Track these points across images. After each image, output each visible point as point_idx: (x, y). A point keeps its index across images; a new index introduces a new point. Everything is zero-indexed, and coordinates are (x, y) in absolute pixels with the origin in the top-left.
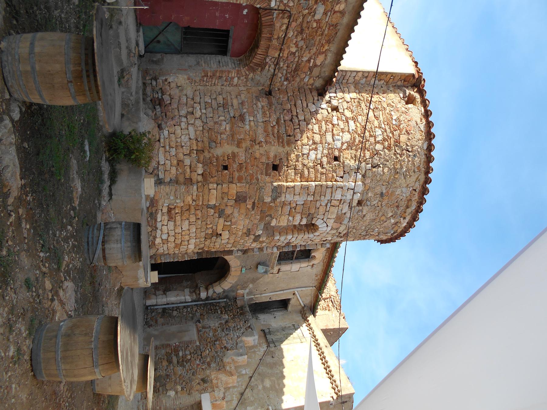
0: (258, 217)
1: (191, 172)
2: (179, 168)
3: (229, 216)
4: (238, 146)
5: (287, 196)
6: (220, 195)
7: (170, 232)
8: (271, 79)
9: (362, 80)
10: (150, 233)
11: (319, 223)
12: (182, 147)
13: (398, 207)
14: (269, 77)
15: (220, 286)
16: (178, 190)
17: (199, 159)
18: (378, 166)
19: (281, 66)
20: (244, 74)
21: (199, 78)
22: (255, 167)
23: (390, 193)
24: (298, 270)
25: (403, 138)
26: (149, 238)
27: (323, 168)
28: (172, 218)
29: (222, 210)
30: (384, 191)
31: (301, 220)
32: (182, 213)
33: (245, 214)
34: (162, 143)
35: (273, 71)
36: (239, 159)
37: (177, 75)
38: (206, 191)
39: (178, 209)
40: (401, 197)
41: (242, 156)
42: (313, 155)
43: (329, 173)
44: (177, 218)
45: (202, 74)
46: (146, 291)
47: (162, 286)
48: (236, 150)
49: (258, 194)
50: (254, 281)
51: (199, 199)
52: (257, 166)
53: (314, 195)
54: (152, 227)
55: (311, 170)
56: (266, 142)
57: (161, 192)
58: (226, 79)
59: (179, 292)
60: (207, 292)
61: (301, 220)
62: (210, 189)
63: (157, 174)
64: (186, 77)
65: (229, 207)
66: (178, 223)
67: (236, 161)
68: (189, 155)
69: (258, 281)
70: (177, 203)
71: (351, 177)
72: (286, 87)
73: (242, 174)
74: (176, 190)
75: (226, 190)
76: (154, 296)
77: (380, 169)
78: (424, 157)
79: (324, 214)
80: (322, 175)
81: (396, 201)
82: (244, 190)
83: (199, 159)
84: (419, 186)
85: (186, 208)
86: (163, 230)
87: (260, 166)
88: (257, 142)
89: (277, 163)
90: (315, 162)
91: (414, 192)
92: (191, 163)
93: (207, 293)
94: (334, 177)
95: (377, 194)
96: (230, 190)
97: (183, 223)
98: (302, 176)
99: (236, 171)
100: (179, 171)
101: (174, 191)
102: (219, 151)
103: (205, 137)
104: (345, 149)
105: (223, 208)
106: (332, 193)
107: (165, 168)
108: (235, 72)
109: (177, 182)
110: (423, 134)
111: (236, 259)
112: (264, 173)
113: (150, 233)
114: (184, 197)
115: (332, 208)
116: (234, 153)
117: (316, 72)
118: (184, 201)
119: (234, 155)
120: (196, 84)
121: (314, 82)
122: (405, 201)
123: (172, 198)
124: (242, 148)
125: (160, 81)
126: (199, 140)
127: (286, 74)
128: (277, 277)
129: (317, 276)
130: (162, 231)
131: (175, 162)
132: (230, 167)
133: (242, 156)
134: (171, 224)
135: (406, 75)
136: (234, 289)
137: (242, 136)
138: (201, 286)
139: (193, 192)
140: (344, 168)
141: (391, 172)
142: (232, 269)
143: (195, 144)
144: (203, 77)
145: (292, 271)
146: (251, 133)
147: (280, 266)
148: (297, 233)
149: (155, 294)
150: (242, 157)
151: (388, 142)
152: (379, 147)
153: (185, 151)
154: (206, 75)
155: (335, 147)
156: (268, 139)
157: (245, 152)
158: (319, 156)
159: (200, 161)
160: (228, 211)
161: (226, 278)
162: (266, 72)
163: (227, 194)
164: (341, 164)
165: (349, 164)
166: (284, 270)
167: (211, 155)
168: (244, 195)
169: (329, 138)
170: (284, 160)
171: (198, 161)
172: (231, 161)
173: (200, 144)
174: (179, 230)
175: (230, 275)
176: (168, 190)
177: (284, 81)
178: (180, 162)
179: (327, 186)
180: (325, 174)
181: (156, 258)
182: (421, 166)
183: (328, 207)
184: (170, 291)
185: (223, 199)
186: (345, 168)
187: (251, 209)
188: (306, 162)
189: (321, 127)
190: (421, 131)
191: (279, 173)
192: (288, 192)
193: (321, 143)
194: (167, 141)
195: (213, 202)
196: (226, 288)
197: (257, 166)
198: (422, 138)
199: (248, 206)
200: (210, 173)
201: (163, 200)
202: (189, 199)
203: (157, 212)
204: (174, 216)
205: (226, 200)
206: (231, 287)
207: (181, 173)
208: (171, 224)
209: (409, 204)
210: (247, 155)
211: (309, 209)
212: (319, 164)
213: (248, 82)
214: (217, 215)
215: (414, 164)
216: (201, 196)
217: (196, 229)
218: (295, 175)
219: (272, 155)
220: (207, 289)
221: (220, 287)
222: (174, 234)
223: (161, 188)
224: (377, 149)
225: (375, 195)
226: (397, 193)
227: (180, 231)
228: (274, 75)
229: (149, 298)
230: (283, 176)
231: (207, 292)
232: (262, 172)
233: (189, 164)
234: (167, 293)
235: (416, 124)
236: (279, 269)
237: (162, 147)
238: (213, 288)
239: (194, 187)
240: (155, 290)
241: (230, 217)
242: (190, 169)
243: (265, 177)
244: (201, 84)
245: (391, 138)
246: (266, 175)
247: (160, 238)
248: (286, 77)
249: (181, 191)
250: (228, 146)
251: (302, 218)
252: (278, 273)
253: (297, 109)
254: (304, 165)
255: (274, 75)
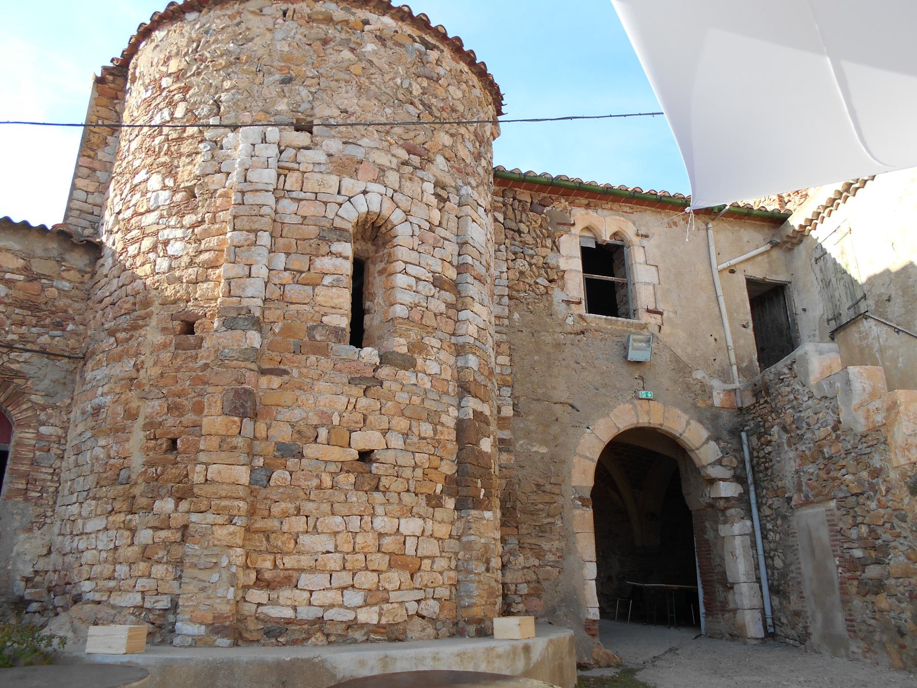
0: (313, 358)
1: (169, 528)
2: (156, 557)
3: (299, 432)
4: (132, 416)
5: (249, 292)
6: (223, 455)
7: (335, 584)
8: (52, 357)
9: (98, 177)
10: (332, 638)
11: (350, 215)
12: (116, 548)
13: (325, 42)
14: (46, 360)
15: (698, 449)
16: (195, 560)
17: (143, 508)
18: (217, 103)
19: (15, 337)
20: (30, 413)
21: (30, 508)
22: (179, 375)
23: (283, 64)
24: (654, 268)
25: (174, 66)
26: (355, 641)
27: (203, 221)
28: (288, 578)
29: (278, 450)
30: (278, 77)
31: (339, 255)
32: (275, 550)
33: (298, 392)
34: (102, 596)
35: (27, 355)
36: (157, 413)
37: (14, 554)
38: (208, 489)
39: (260, 561)
40: (298, 36)
41: (153, 407)
42: (175, 248)
43: (215, 205)
44: (288, 566)
45: (19, 502)
46: (731, 635)
47: (718, 591)
48: (141, 421)
49: (235, 362)
50: (682, 368)
51: (225, 507)
52: (178, 370)
53: (256, 232)
54: (311, 632)
55: (202, 247)
56: (137, 354)
57: (195, 606)
58: (40, 449)
59: (725, 550)
60: (720, 480)
61: (339, 255)
62: (207, 480)
63: (161, 612)
64: (22, 536)
65: (272, 432)
66: (306, 561)
67: (161, 420)
68: (133, 531)
69: (685, 359)
70: (230, 563)
71: (228, 156)
72: (81, 324)
73: (187, 403)
74: (194, 566)
75: (215, 441)
76: (739, 615)
77: (224, 96)
78: (212, 13)
79: (325, 203)
80: (217, 220)
81: (307, 47)
82: (218, 397)
83: (143, 508)
84: (274, 6)
85: (261, 542)
86: (327, 602)
87: (178, 362)
88: (134, 375)
89: (177, 325)
90: (190, 239)
91: (290, 13)
92: (150, 528)
93: (724, 480)
94: (226, 192)
95: (283, 91)
96: (213, 432)
97: (307, 548)
98: (213, 264)
99: (182, 419)
100: (163, 557)
101: (196, 573)
102: (137, 461)
103: (108, 494)
104: (175, 182)
105: (271, 449)
106: (257, 191)
107: (150, 593)
108: (22, 432)
109: (179, 563)
110: (173, 28)
111: (611, 415)
112: (194, 352)
113: (332, 638)
114: (215, 546)
115: (308, 186)
116: (144, 425)
117: (38, 267)
118: (228, 546)
119: (150, 425)
120: (49, 514)
121: (73, 268)
122: (312, 27)
123: (215, 577)
124: (139, 407)
125: (28, 593)
126: (109, 508)
127: (43, 326)
128: (672, 315)
129: (675, 224)
130: (332, 606)
131: (142, 566)
132: (170, 432)
133: (153, 407)
134: (305, 580)
135: (97, 95)
136: (710, 418)
137: (120, 409)
138: (708, 495)
139: (206, 522)
140: (207, 175)
141: (233, 72)
142: (643, 421)
143: (114, 518)
144: (27, 499)
145: (656, 281)
146: (117, 390)
147: (640, 311)
148: (395, 264)
149: (735, 611)
150: (153, 407)
151: (174, 95)
152: (180, 112)
153: (125, 541)
154: (24, 492)
155: (168, 202)
156: (132, 351)
157: (147, 401)
158: (179, 233)
159: (148, 505)
160: (283, 433)
161: (675, 436)
162: (28, 367)
163: (223, 438)
164: (199, 183)
165: (199, 166)
166: (653, 299)
167: (140, 481)
168: (231, 395)
169: (151, 218)
170: (173, 309)
171: (149, 509)
172: (158, 432)
173: (117, 505)
174: (333, 562)
175: (662, 425)
176: (191, 587)
177: (64, 330)
178: (146, 555)
179: (240, 204)
180: (215, 213)
181: (465, 621)
182: (229, 12)
183: (302, 195)
184: (725, 572)
185: (236, 448)
186: (207, 172)
187: (286, 377)
188: (186, 260)
189: (133, 239)
190: (168, 34)
191: (198, 317)
192: (239, 292)
193: (156, 233)
194: (101, 583)
195: (242, 474)
196: (705, 434)
197: (178, 370)
198: (180, 27)
199: (275, 386)
200: (177, 480)
201: (218, 601)
202: (222, 533)
203: (262, 616)
204: (282, 574)
205: (239, 441)
206: (701, 422)
207: (168, 551)
208: (305, 580)
209: (321, 17)
210: (152, 395)
211: (304, 240)
212: (193, 231)
213: (58, 404)
214: (291, 462)
215: (223, 29)
216: (218, 502)
217: (333, 514)
218: (209, 280)
219: (159, 338)
220: (712, 481)
221: (702, 450)
222: (344, 573)
223: (184, 606)
224: (183, 114)
225: (285, 96)
226: (286, 49)
227: (338, 556)
228: (43, 352)
229: (743, 627)
230: (207, 307)
231: (720, 480)
232: (191, 357)
233: (150, 531)
234: (730, 580)
235: (158, 49)
236: (648, 311)
237: (109, 597)
238: (704, 467)
239: (193, 520)
240: (726, 611)
241: (304, 429)
242: (162, 529)
243: (203, 349)
244: (51, 503)
245: (169, 91)
246: (200, 347)
247: (359, 610)
248: (51, 327)
249: (198, 553)
250: (131, 442)
251: (330, 253)
252: (661, 313)
253: (105, 295)
254: (191, 264)
255: (43, 352)
